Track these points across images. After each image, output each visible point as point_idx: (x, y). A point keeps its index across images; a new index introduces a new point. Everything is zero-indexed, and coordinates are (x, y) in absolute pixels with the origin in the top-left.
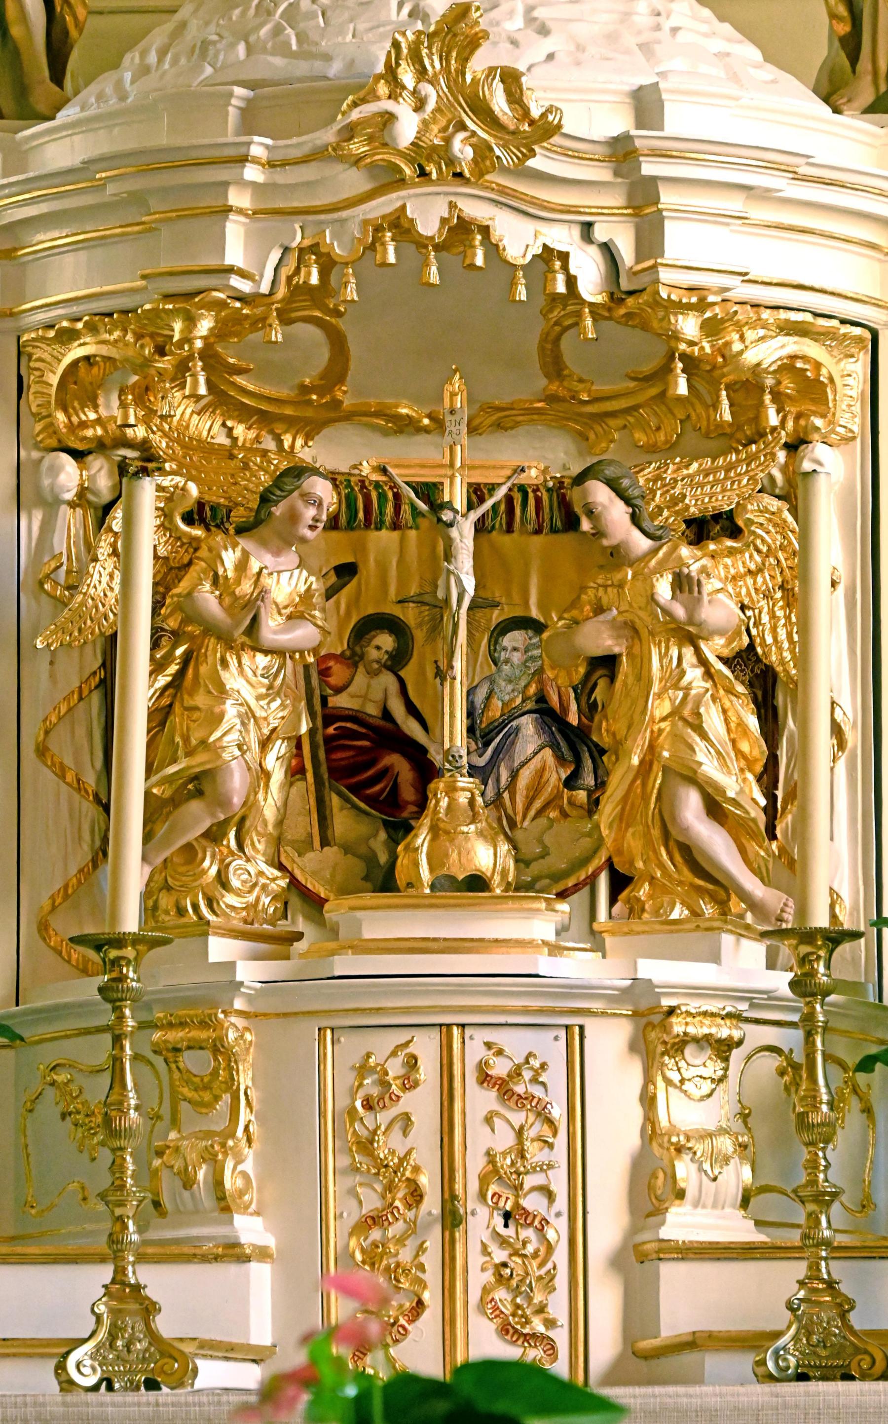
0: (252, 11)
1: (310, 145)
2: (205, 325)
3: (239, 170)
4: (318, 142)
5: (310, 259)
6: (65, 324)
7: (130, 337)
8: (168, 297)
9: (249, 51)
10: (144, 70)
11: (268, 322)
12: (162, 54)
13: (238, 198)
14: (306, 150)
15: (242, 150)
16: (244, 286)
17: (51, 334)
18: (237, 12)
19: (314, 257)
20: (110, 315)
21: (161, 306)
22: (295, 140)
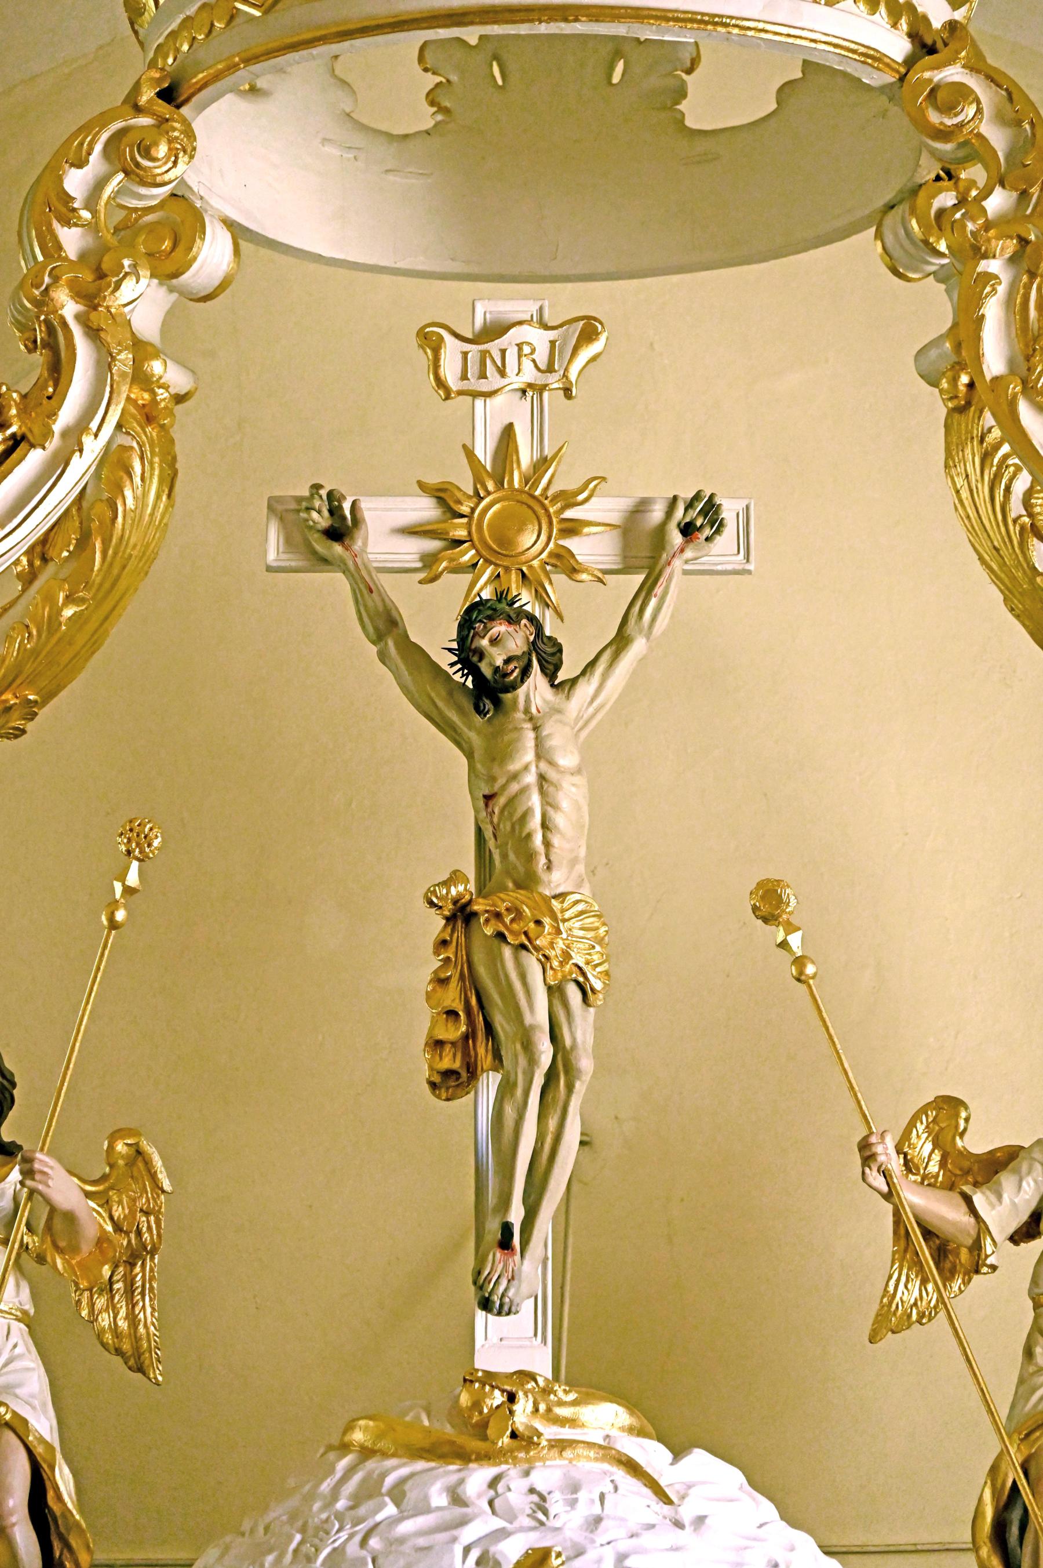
18: (270, 1559)
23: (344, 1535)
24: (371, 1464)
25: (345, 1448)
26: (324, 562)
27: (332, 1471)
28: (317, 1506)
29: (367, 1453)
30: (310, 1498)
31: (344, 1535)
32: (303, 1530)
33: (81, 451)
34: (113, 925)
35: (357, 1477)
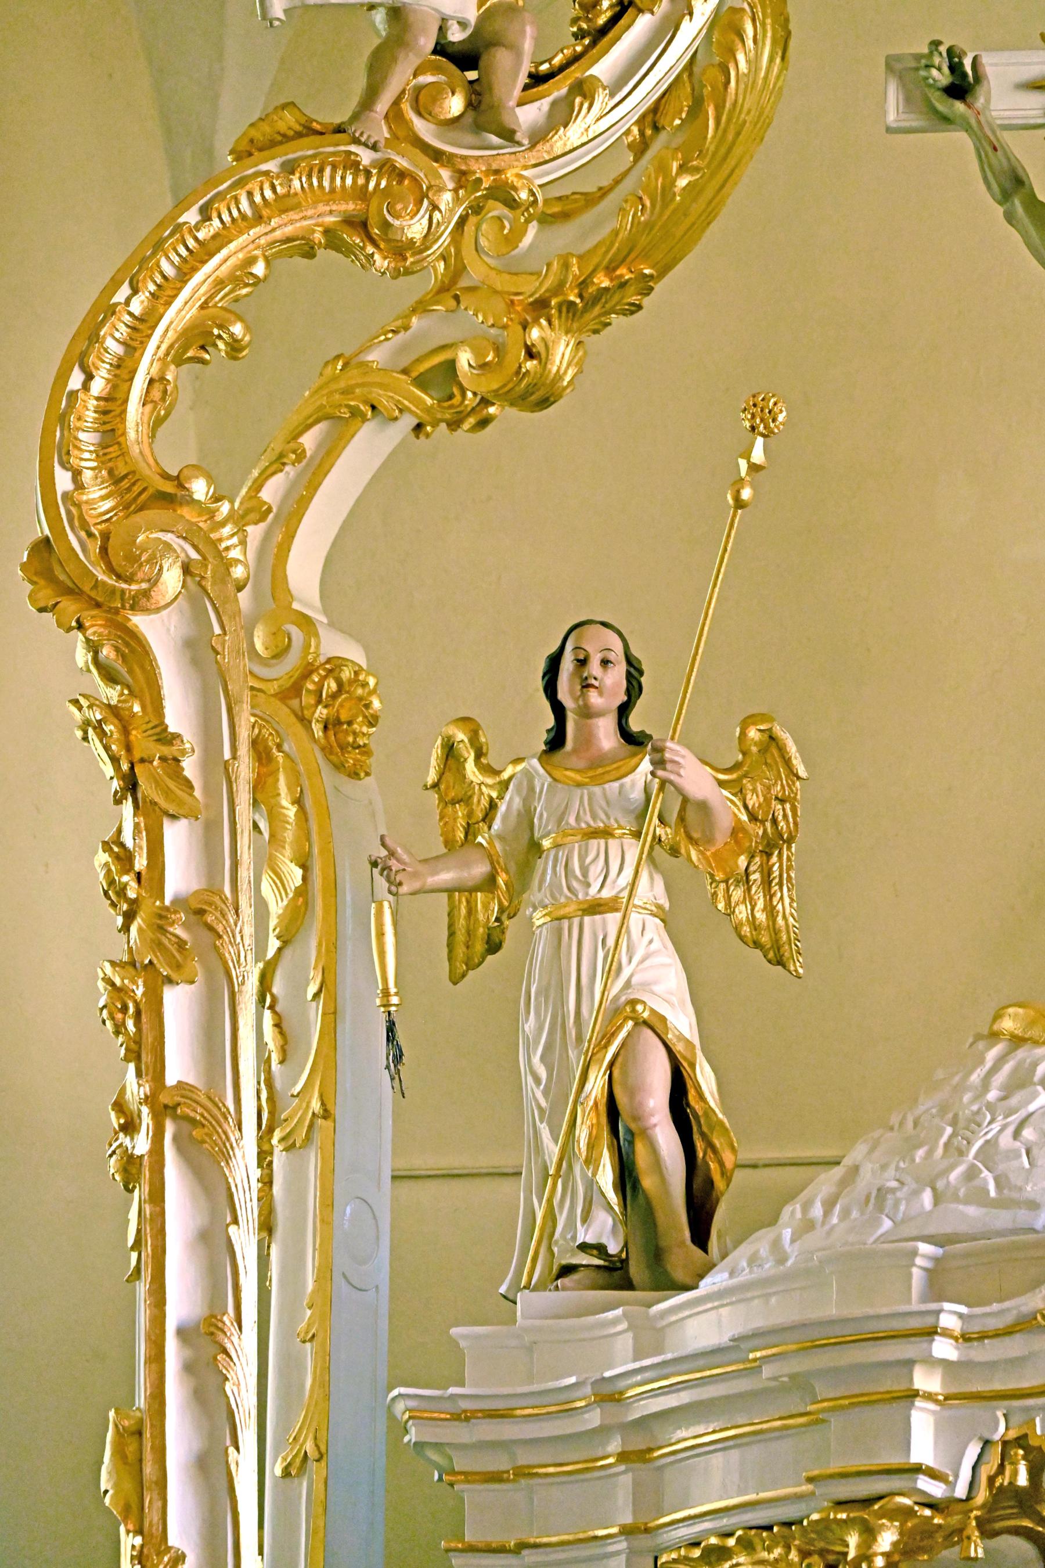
0: (940, 1151)
1: (1015, 1312)
2: (887, 1539)
3: (925, 1345)
4: (1025, 1309)
5: (1016, 1454)
6: (713, 1540)
7: (794, 1556)
8: (840, 1504)
9: (937, 1200)
10: (808, 1226)
11: (965, 1534)
12: (829, 1206)
13: (926, 1381)
14: (1009, 1319)
15: (929, 1321)
16: (936, 1490)
17: (697, 1553)
18: (920, 1153)
19: (1021, 1452)
20: (769, 1528)
21: (832, 1516)
22: (995, 1307)
23: (996, 1127)
24: (1021, 1053)
25: (994, 1036)
26: (946, 120)
27: (981, 1061)
28: (967, 1097)
29: (1017, 1041)
30: (960, 1089)
31: (996, 1127)
32: (954, 1123)
33: (691, 14)
34: (739, 504)
35: (1007, 1068)
